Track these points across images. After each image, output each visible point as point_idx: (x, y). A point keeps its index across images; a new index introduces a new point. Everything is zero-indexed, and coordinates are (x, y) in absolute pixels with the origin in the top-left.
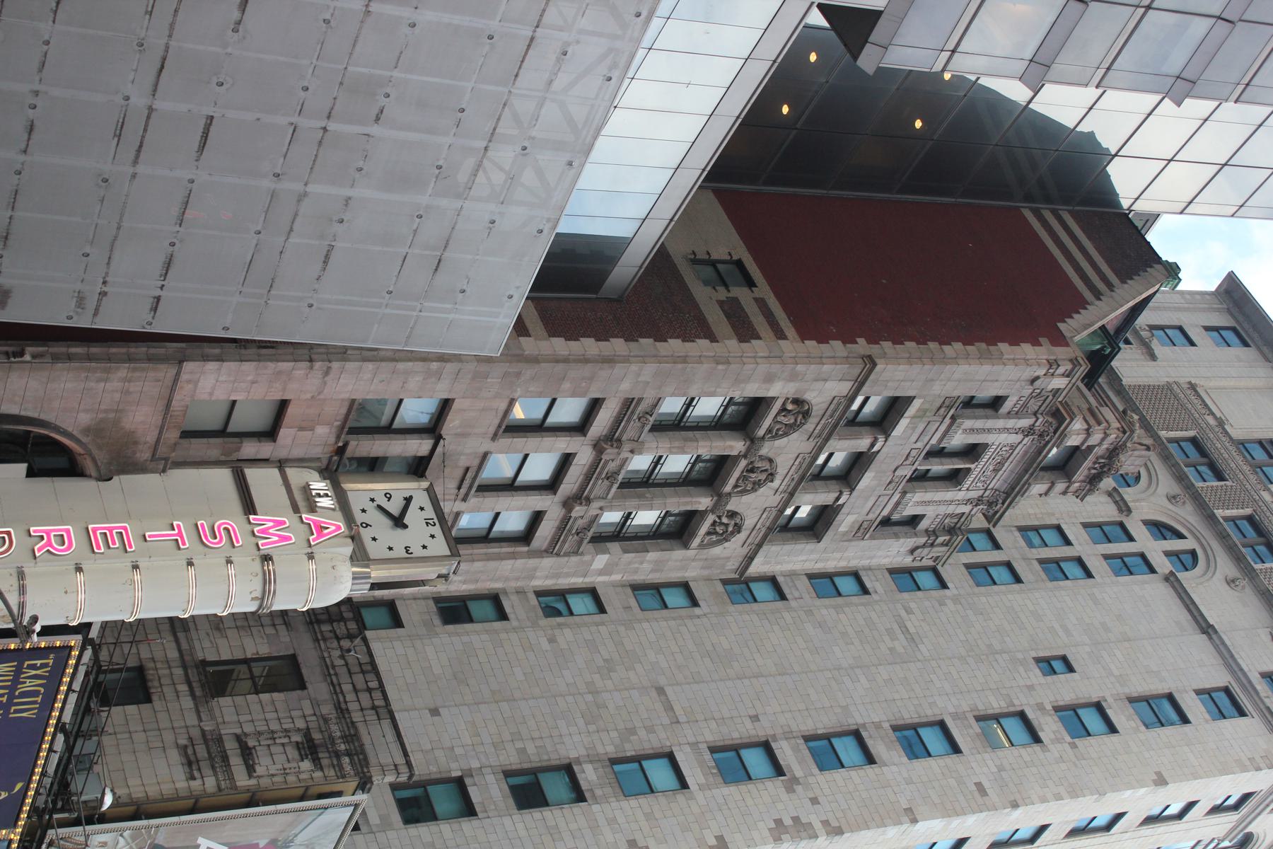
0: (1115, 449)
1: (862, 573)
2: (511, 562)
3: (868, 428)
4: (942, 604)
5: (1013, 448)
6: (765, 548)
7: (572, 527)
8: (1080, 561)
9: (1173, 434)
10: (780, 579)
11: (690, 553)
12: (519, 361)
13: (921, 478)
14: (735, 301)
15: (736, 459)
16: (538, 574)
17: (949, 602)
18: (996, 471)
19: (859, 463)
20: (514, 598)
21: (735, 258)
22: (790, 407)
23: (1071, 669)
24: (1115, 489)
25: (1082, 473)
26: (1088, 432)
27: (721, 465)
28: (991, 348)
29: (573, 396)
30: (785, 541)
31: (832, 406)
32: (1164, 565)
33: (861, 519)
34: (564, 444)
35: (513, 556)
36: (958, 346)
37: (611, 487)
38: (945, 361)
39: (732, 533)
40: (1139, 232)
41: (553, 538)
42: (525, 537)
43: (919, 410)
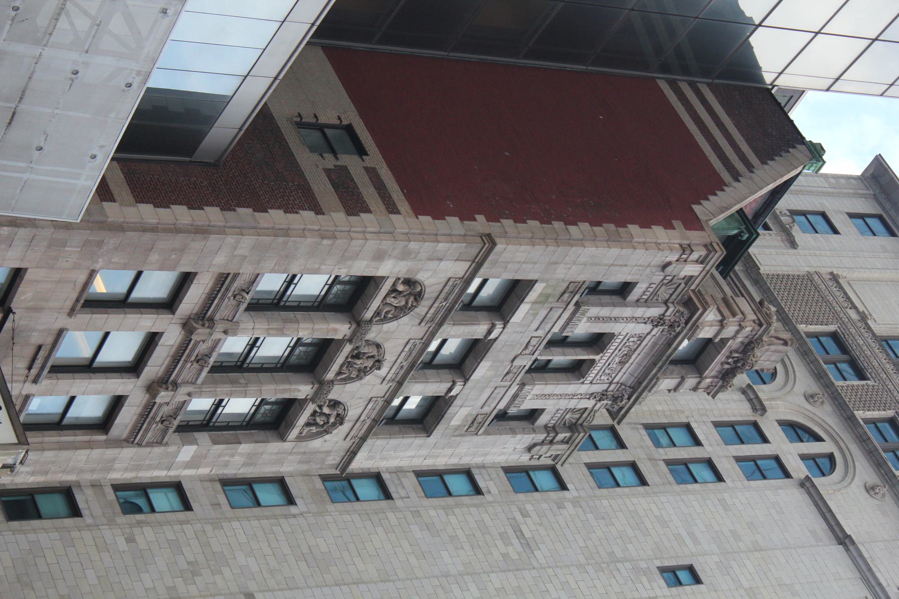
0: (751, 342)
1: (475, 472)
2: (87, 451)
3: (485, 313)
4: (560, 506)
5: (641, 338)
6: (369, 442)
7: (156, 414)
8: (710, 463)
9: (812, 328)
10: (386, 476)
11: (287, 446)
12: (101, 229)
13: (541, 369)
14: (344, 169)
15: (340, 343)
16: (117, 466)
17: (568, 505)
18: (622, 363)
19: (474, 350)
20: (89, 492)
21: (345, 122)
22: (401, 288)
23: (697, 580)
24: (749, 386)
25: (714, 368)
26: (722, 324)
27: (323, 349)
28: (621, 230)
29: (161, 269)
30: (391, 435)
31: (447, 288)
32: (798, 469)
33: (475, 413)
34: (149, 322)
35: (89, 445)
36: (585, 226)
37: (201, 370)
38: (571, 242)
40: (782, 109)
41: (135, 426)
42: (104, 424)
43: (541, 295)
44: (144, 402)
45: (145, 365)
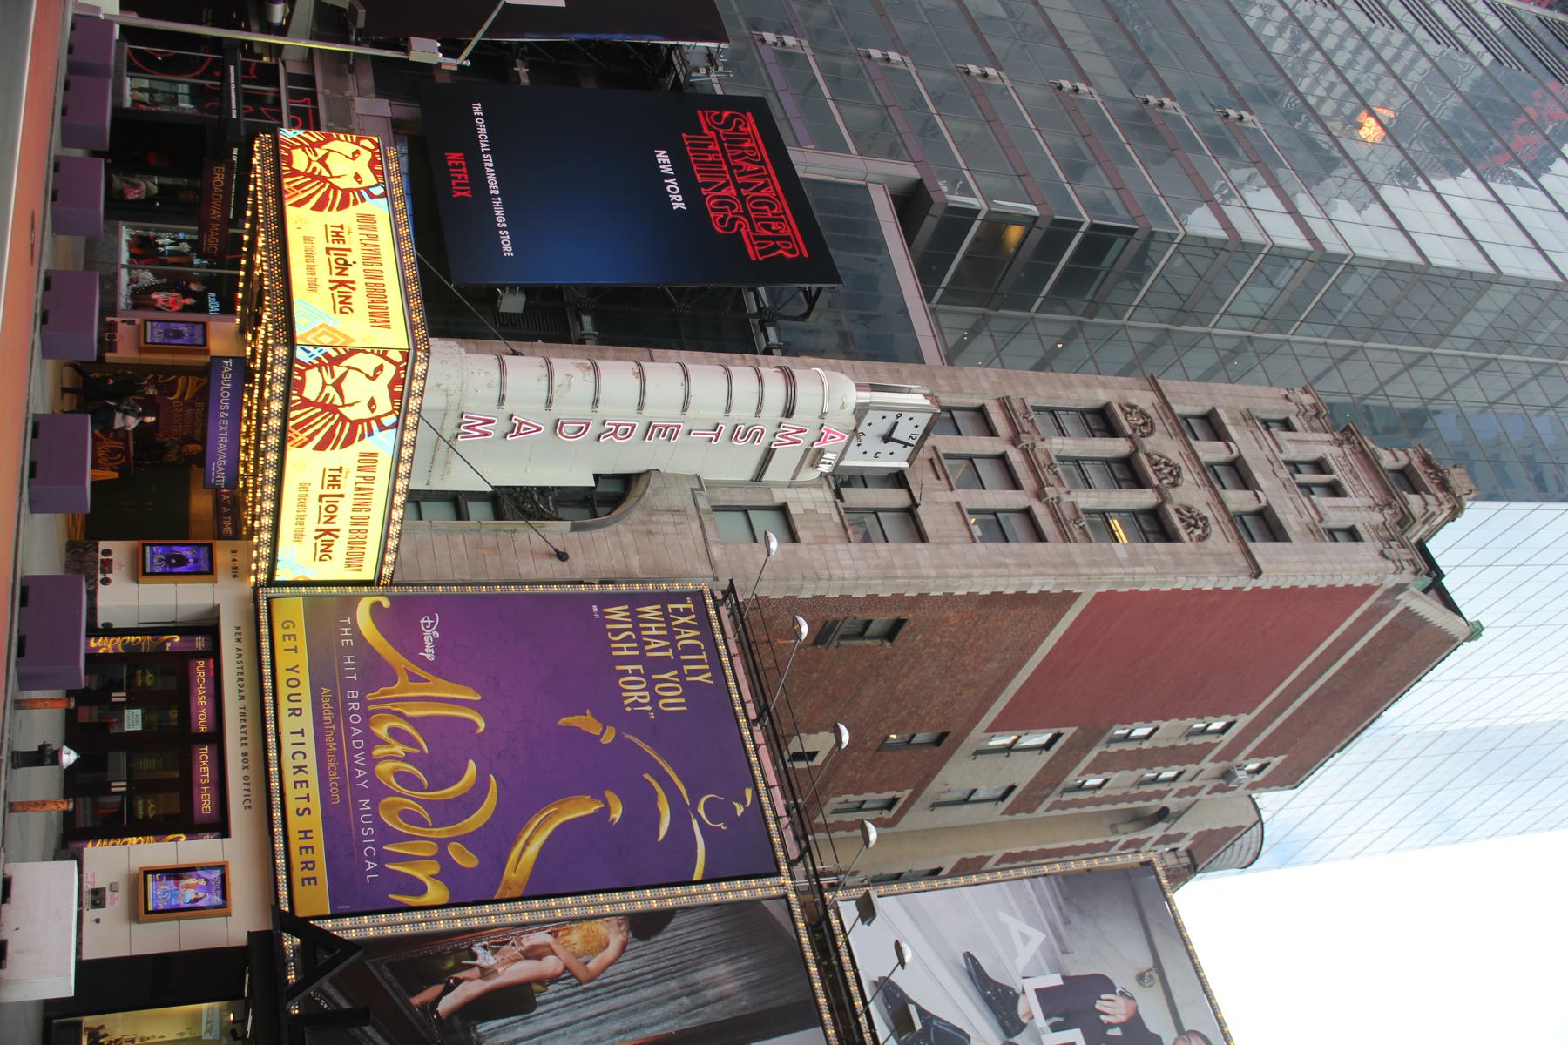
16: (1079, 560)
18: (1357, 478)
39: (1206, 526)
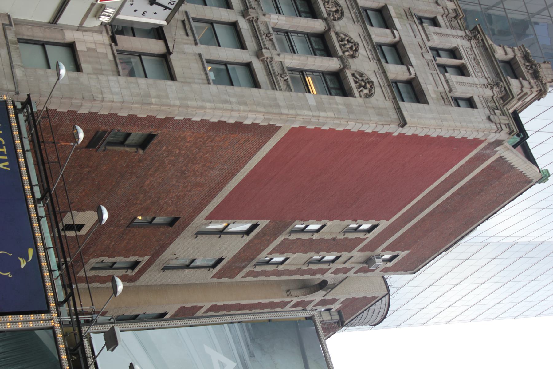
7: (273, 70)
16: (282, 103)
18: (478, 64)
39: (372, 87)
41: (270, 82)
44: (263, 67)
45: (245, 42)
